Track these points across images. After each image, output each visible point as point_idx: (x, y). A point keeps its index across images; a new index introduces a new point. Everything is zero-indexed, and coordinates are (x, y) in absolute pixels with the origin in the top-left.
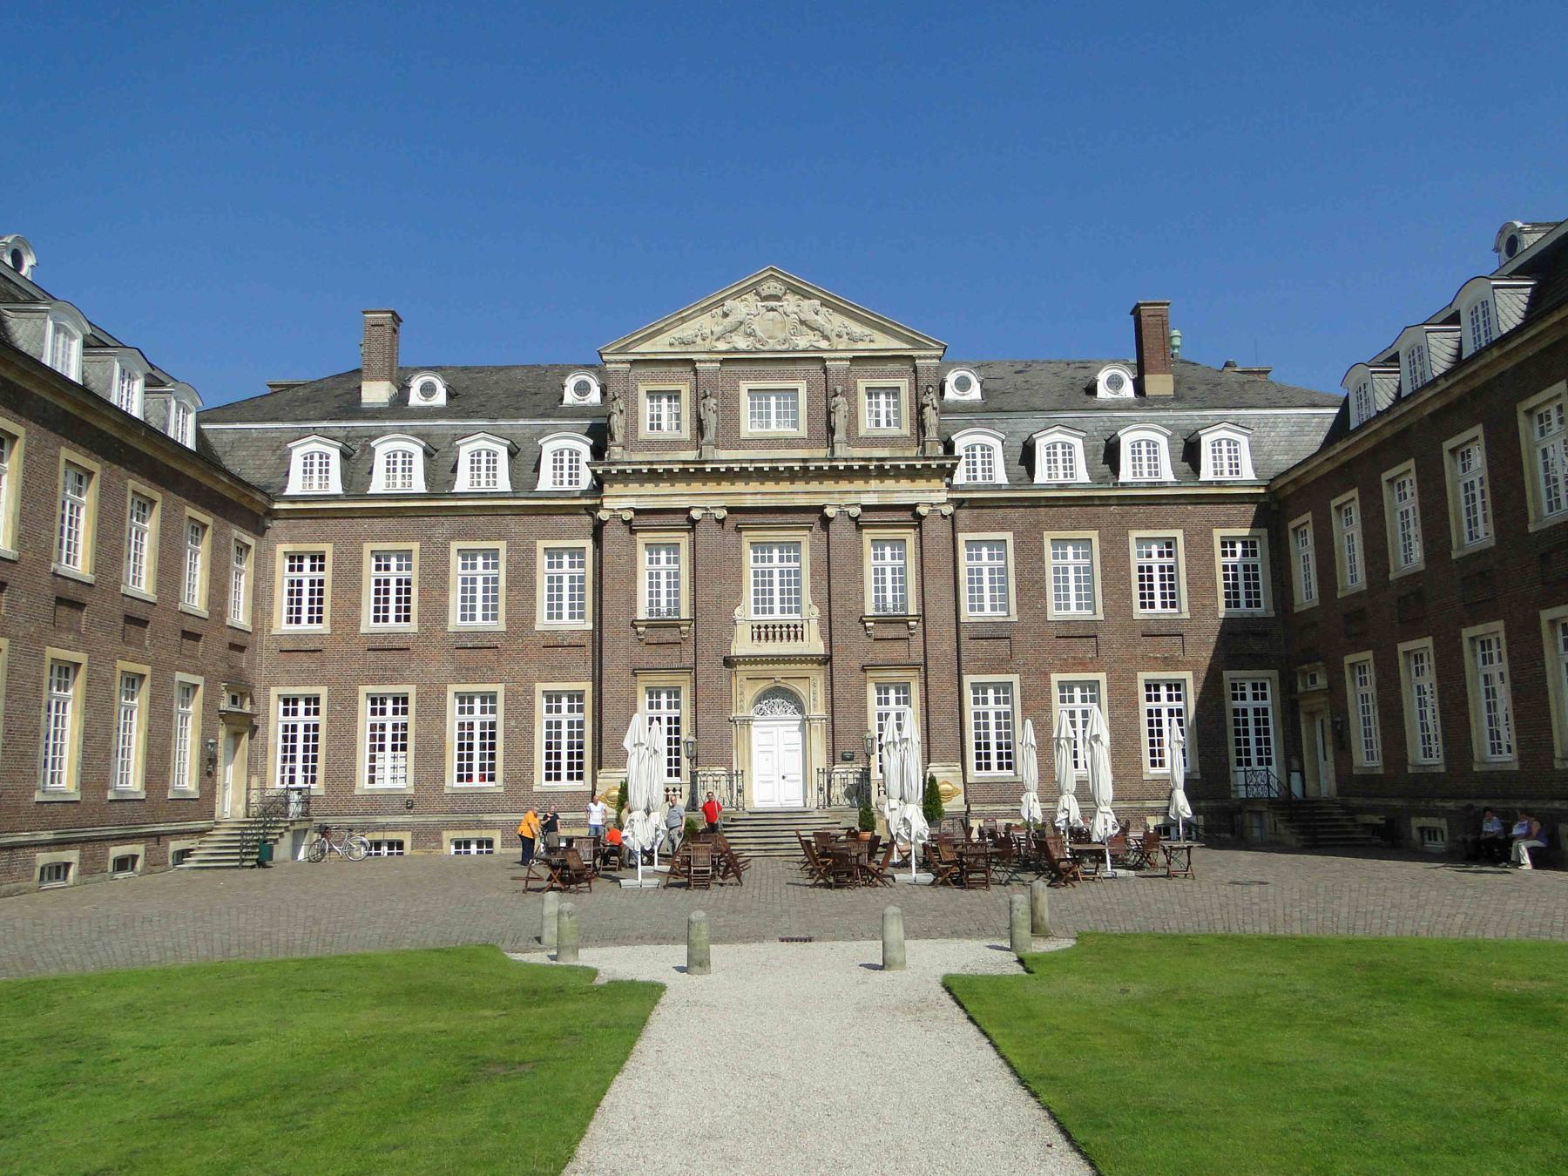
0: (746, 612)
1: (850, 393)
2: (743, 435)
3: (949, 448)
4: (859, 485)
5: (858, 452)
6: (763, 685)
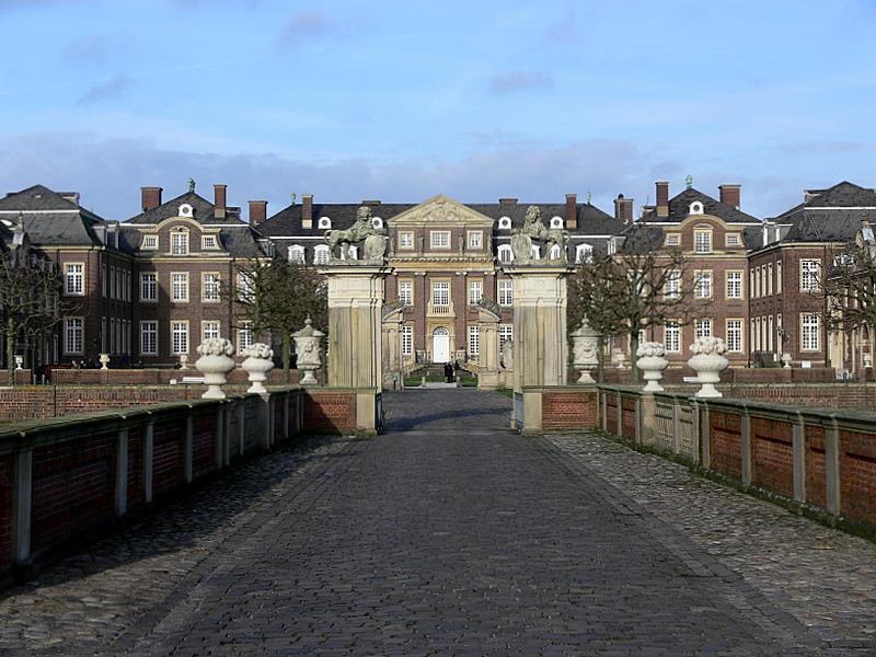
0: (430, 305)
1: (464, 236)
2: (431, 247)
3: (495, 252)
4: (465, 265)
5: (467, 254)
6: (437, 326)
